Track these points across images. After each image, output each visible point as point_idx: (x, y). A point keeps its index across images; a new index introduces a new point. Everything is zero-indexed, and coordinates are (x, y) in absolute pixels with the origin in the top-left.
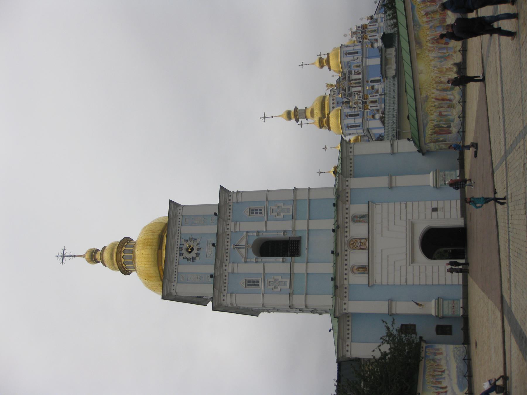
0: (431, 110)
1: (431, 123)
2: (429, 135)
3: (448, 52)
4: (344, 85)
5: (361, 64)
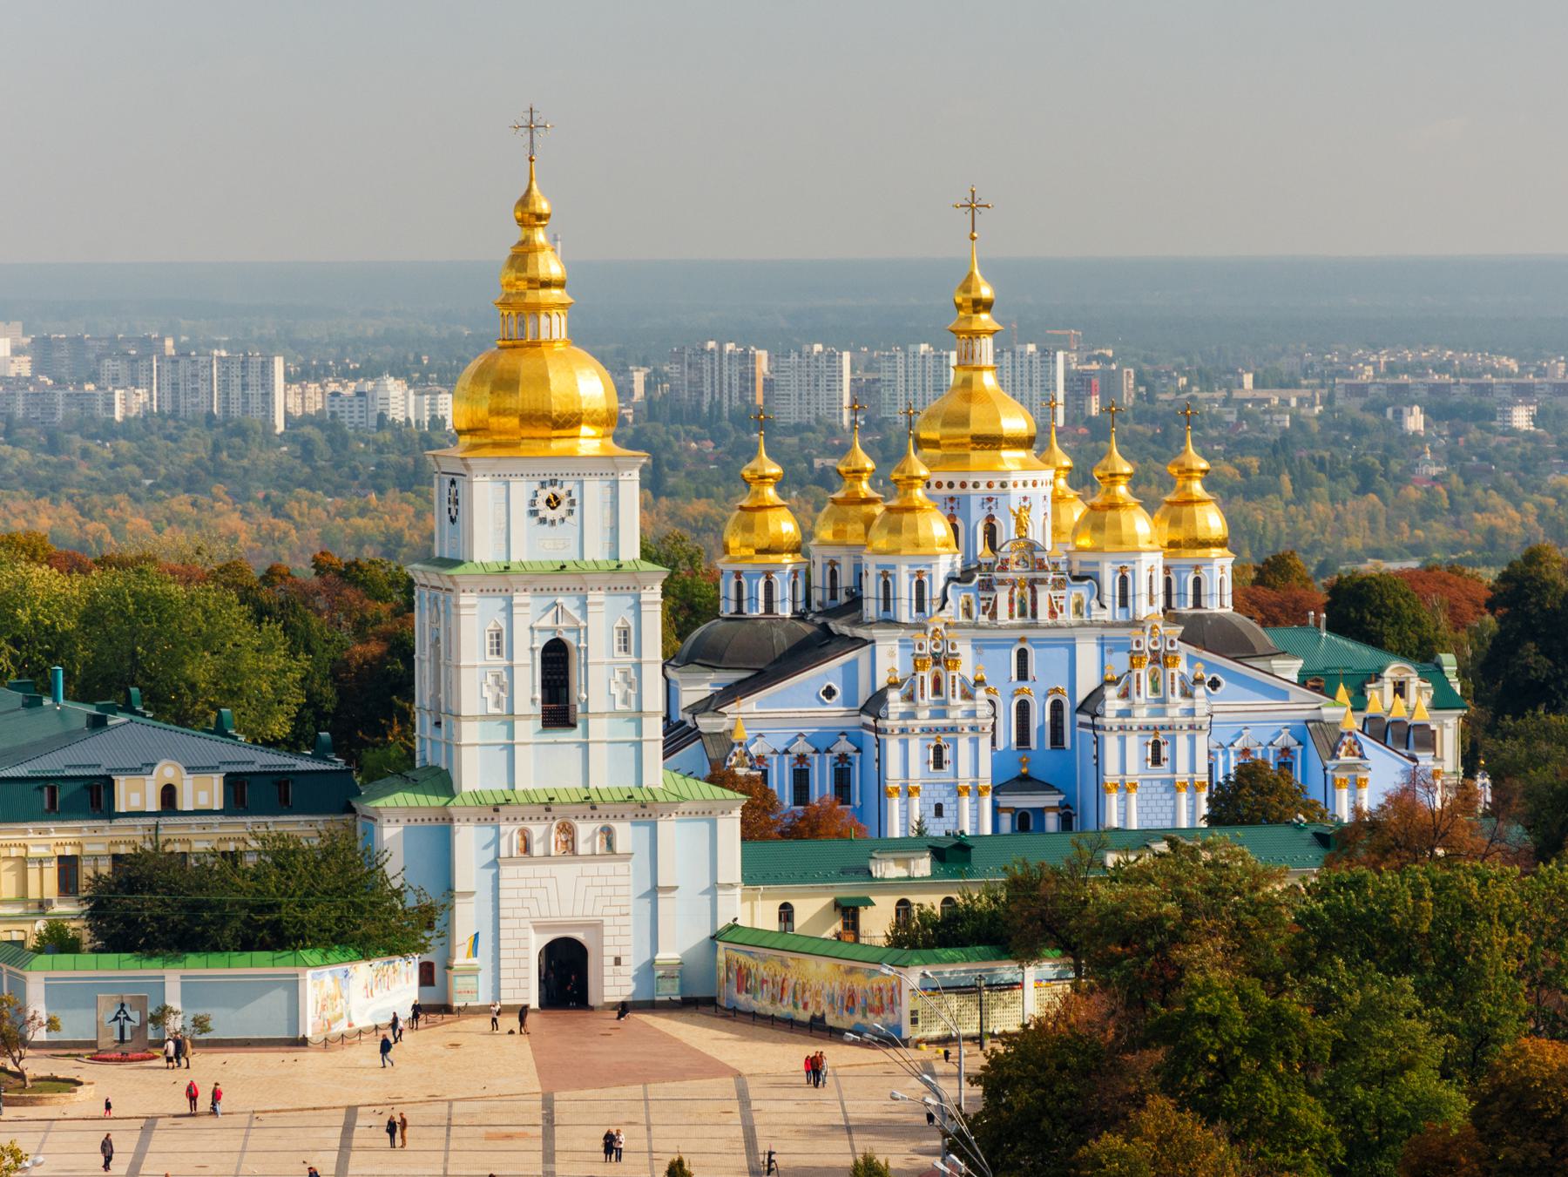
5: (1085, 618)
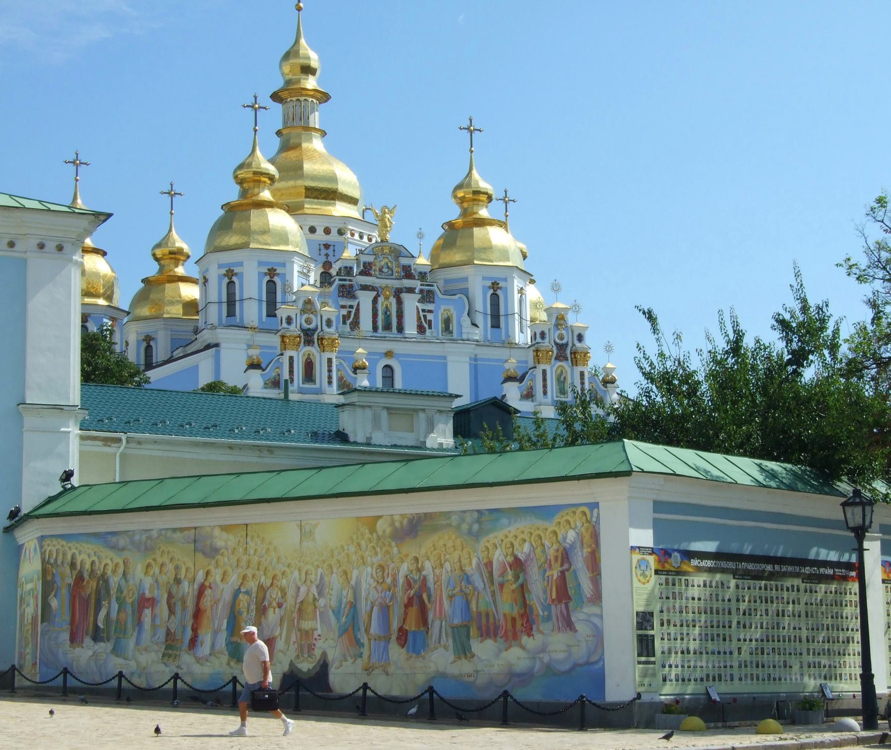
0: (162, 565)
1: (117, 565)
2: (73, 557)
3: (369, 640)
4: (385, 270)
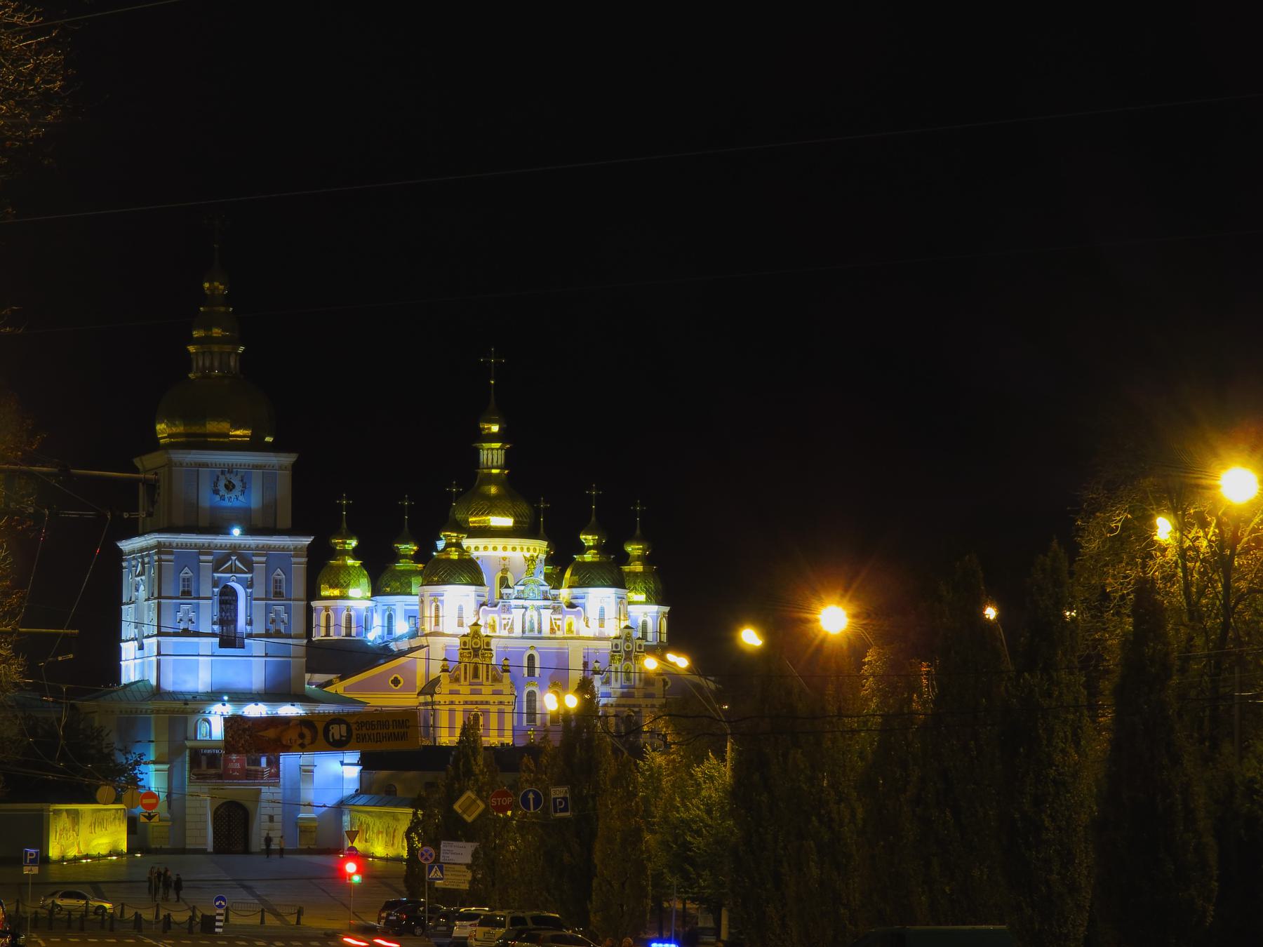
4: (531, 594)
5: (574, 635)
